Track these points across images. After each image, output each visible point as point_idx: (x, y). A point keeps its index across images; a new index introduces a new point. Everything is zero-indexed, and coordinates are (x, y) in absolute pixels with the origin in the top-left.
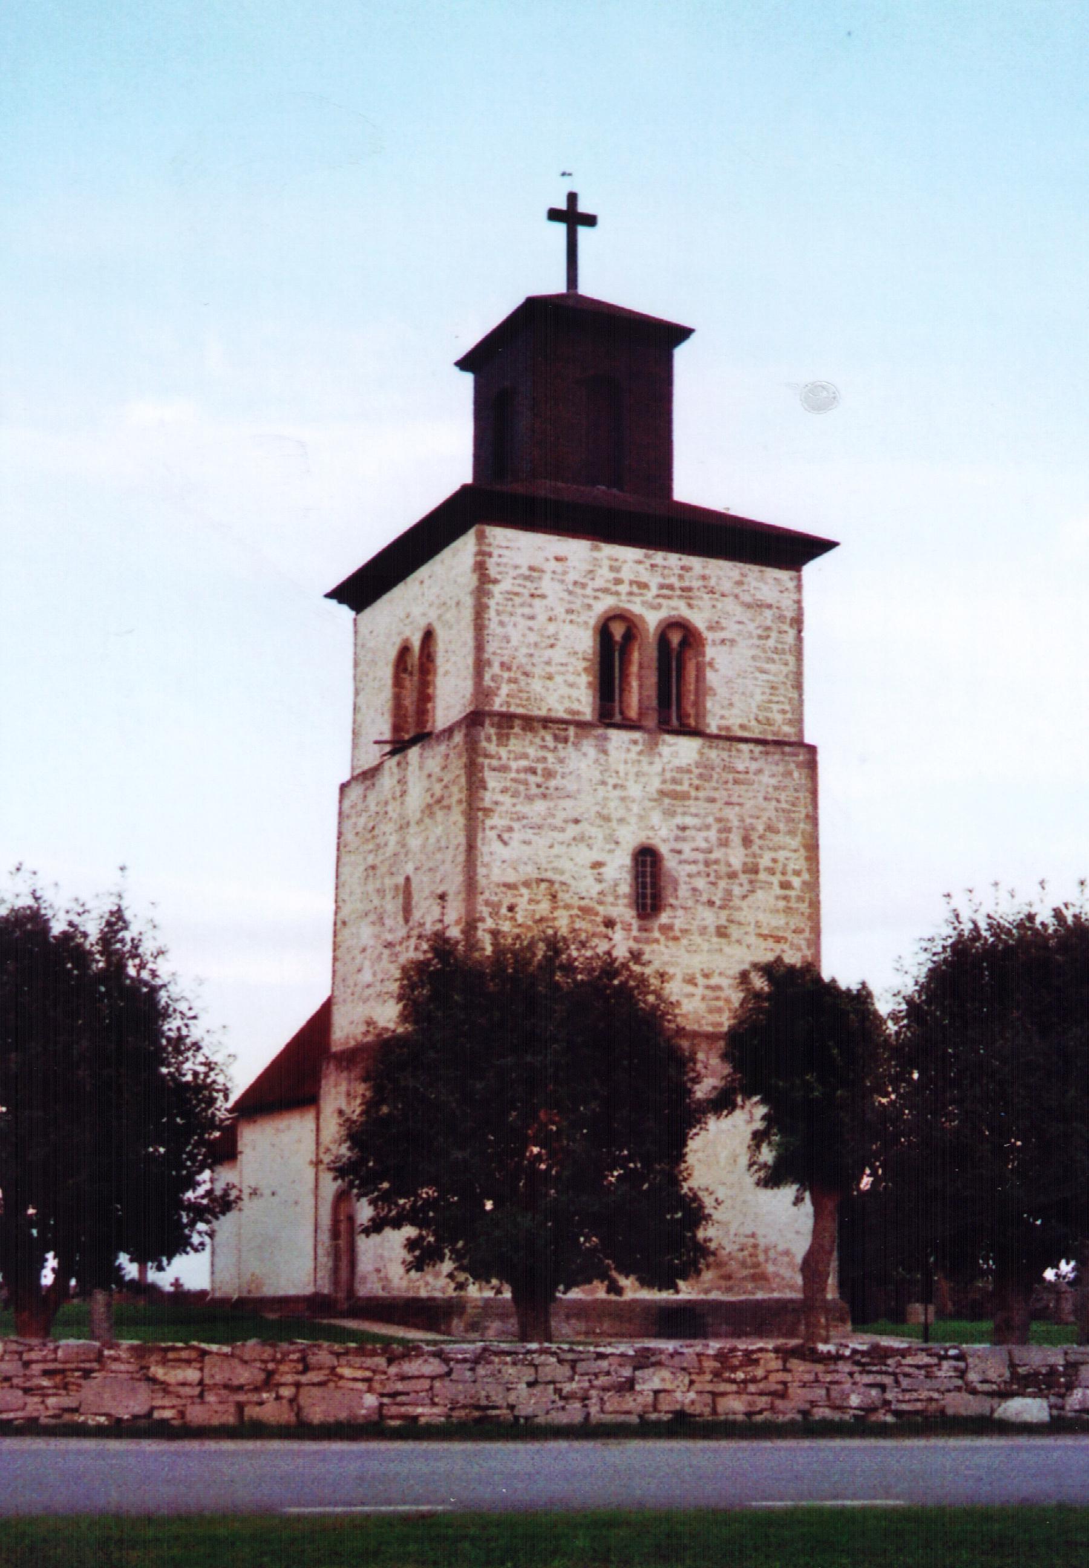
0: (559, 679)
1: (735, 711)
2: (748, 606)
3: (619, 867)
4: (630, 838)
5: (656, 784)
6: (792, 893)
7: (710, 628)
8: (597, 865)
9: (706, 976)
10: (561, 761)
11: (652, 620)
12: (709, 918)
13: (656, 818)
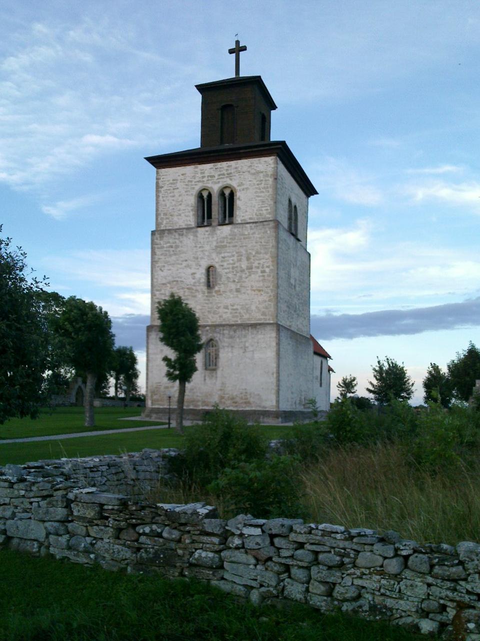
0: (182, 215)
1: (247, 214)
2: (254, 174)
3: (201, 274)
4: (205, 264)
5: (215, 244)
6: (266, 274)
7: (238, 186)
9: (233, 306)
10: (181, 242)
11: (215, 188)
13: (214, 255)
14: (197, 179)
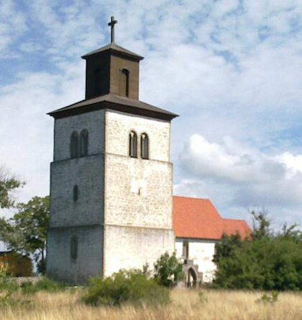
4: (73, 184)
8: (68, 191)
11: (79, 131)
12: (85, 199)
14: (72, 126)
